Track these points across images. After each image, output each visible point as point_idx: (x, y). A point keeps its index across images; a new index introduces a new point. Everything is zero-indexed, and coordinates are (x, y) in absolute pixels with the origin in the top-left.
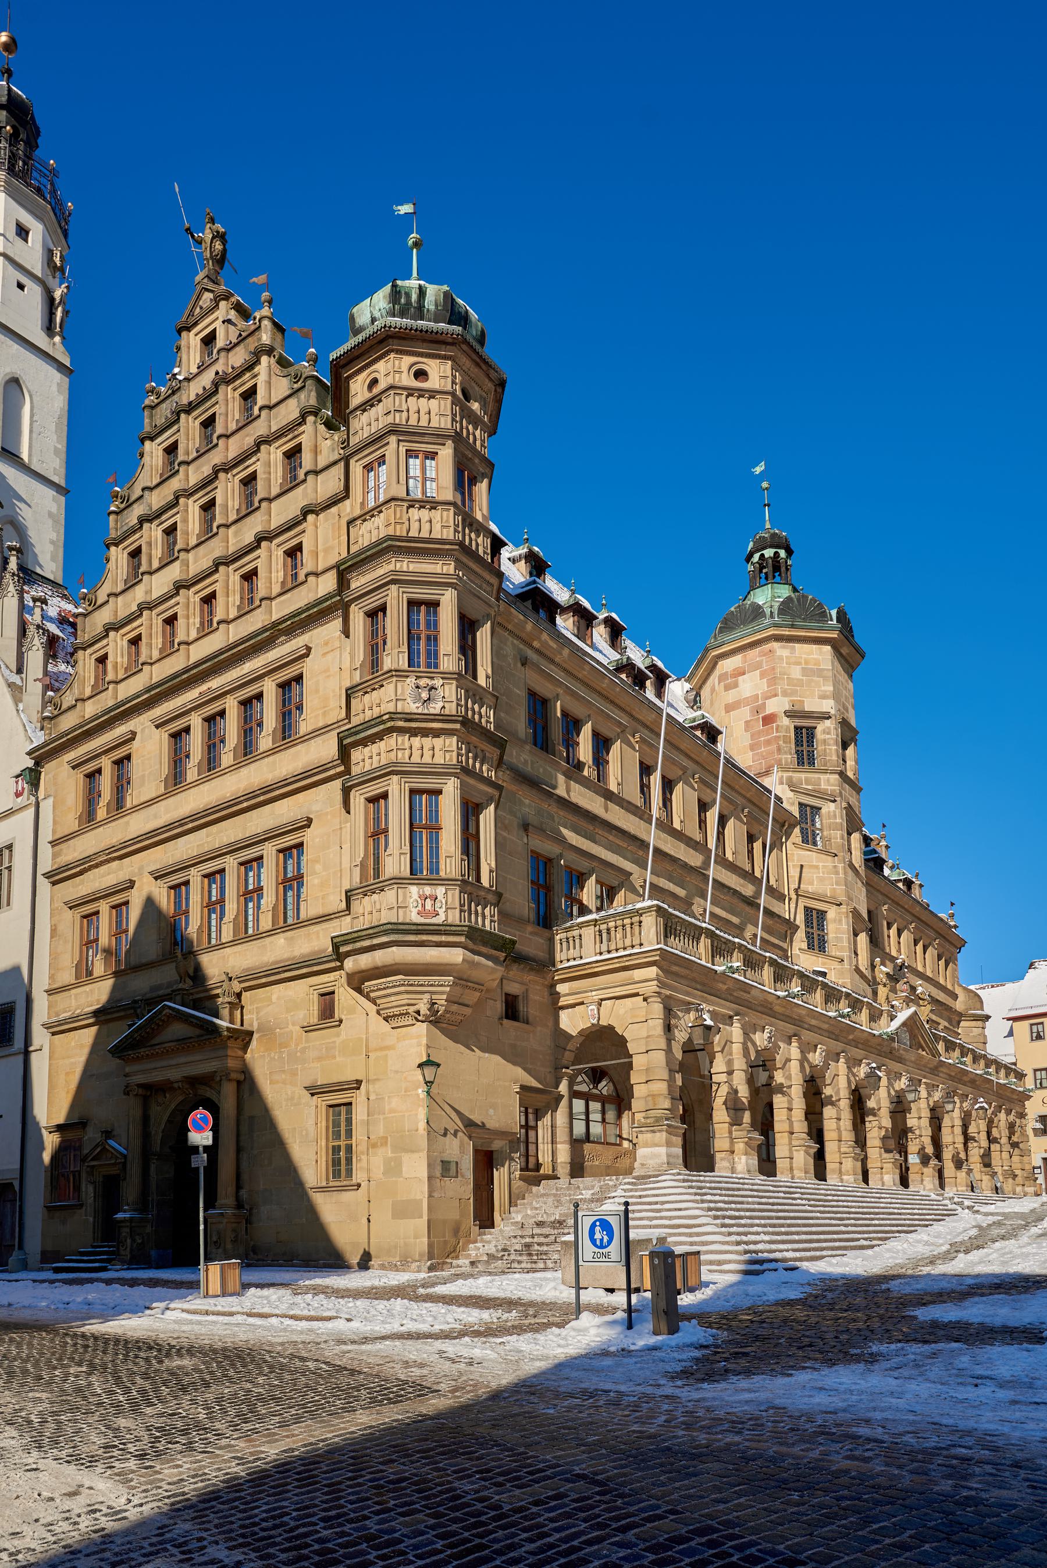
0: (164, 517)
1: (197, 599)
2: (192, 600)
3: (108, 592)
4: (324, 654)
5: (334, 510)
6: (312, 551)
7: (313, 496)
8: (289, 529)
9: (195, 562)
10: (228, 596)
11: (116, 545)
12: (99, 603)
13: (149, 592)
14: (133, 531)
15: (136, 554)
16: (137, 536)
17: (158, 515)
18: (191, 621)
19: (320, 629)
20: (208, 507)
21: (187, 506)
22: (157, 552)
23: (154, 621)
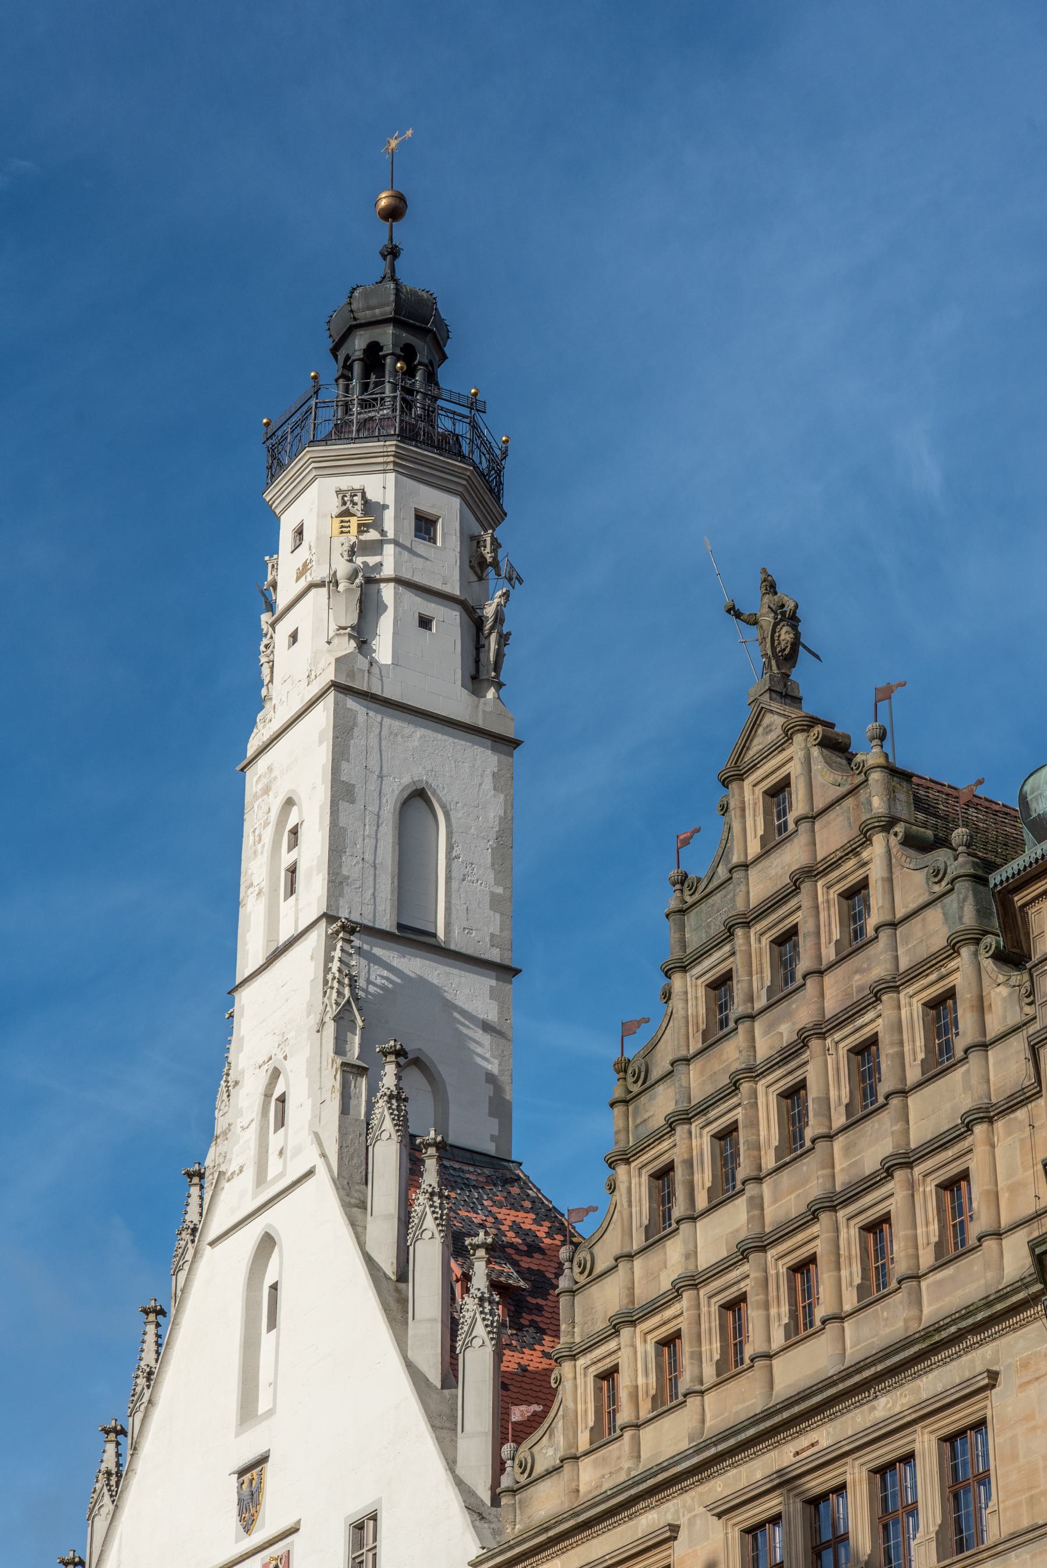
0: (713, 1114)
1: (783, 1270)
2: (772, 1272)
3: (617, 1251)
4: (1023, 1386)
5: (1021, 1114)
6: (988, 1192)
7: (979, 1089)
8: (943, 1147)
9: (775, 1200)
10: (839, 1269)
11: (627, 1162)
12: (599, 1268)
13: (691, 1254)
14: (658, 1137)
15: (663, 1174)
16: (665, 1145)
17: (704, 1108)
18: (773, 1311)
19: (1011, 1337)
20: (794, 1094)
21: (754, 1094)
22: (704, 1178)
23: (704, 1309)
